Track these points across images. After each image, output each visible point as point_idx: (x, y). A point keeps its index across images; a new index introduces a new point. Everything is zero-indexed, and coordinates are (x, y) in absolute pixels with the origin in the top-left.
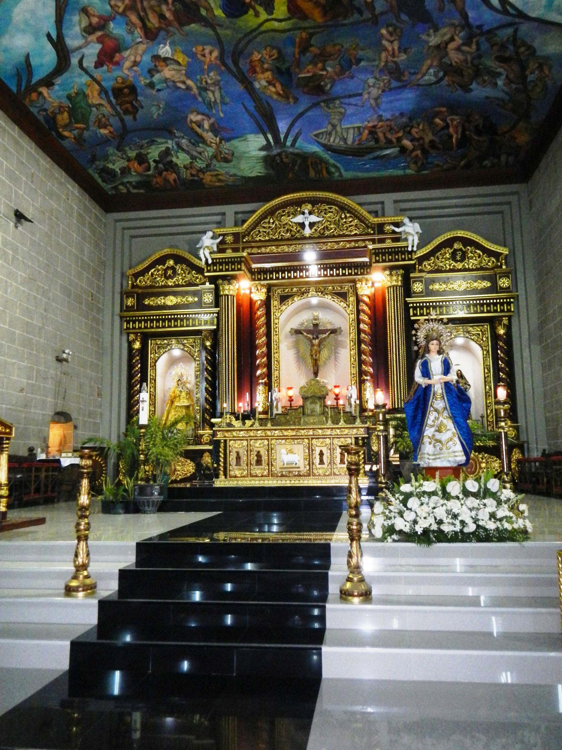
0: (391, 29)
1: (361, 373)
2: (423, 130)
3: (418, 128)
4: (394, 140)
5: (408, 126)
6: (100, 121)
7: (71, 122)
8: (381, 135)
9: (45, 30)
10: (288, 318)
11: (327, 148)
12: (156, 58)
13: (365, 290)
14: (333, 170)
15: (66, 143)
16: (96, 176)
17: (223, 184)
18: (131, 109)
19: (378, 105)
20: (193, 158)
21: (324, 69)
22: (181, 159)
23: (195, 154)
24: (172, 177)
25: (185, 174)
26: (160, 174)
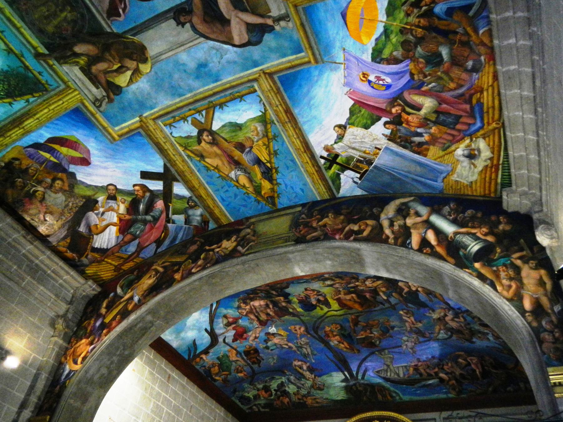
0: (405, 311)
2: (452, 367)
3: (447, 365)
4: (433, 374)
5: (440, 365)
6: (237, 369)
7: (220, 371)
8: (422, 371)
9: (204, 327)
11: (386, 380)
12: (268, 334)
14: (394, 395)
15: (216, 384)
16: (237, 402)
17: (320, 405)
18: (256, 361)
19: (414, 352)
20: (298, 387)
21: (371, 333)
22: (291, 389)
23: (299, 384)
24: (286, 400)
25: (295, 399)
26: (279, 398)
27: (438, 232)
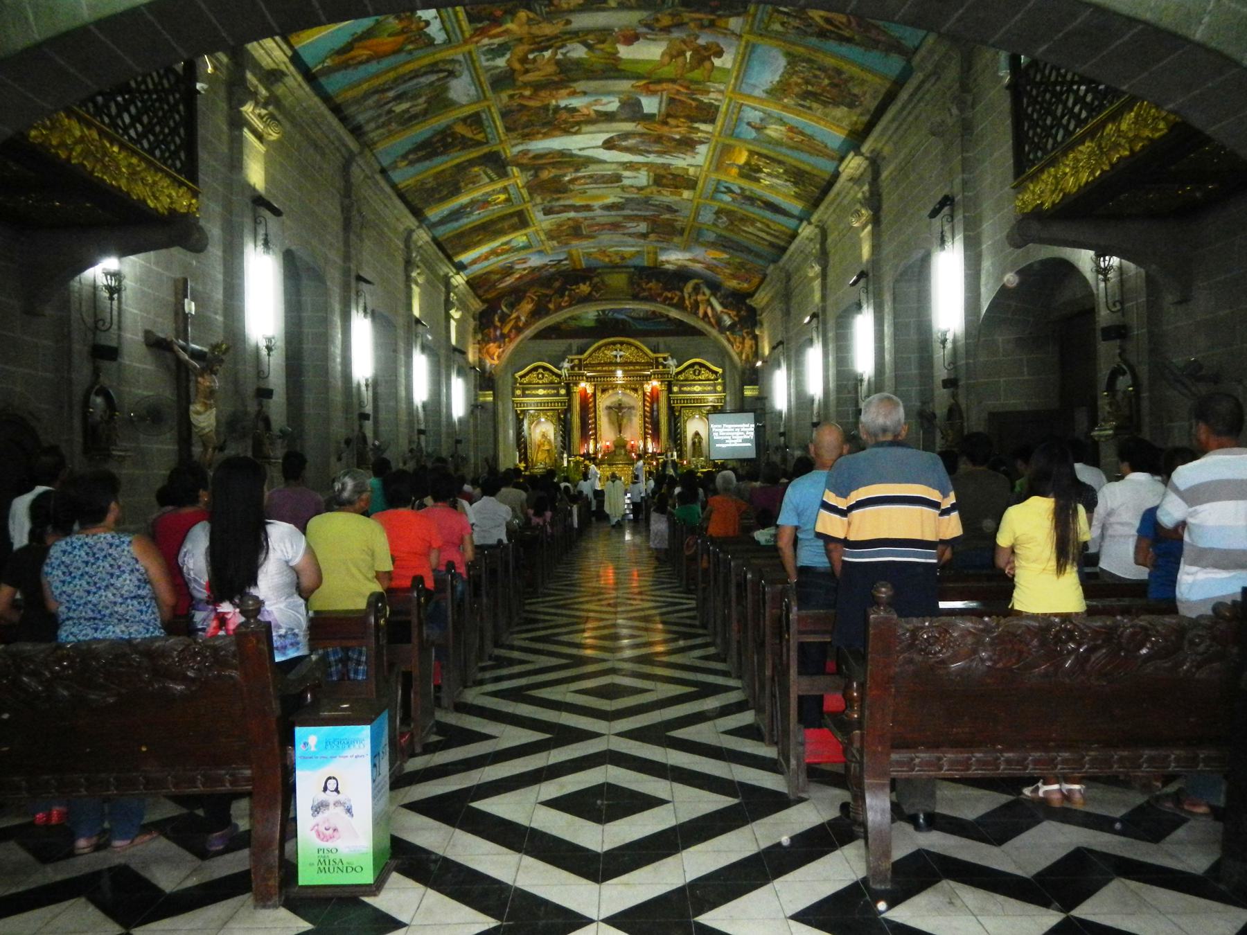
1: (646, 433)
10: (604, 401)
13: (648, 388)
27: (713, 308)
